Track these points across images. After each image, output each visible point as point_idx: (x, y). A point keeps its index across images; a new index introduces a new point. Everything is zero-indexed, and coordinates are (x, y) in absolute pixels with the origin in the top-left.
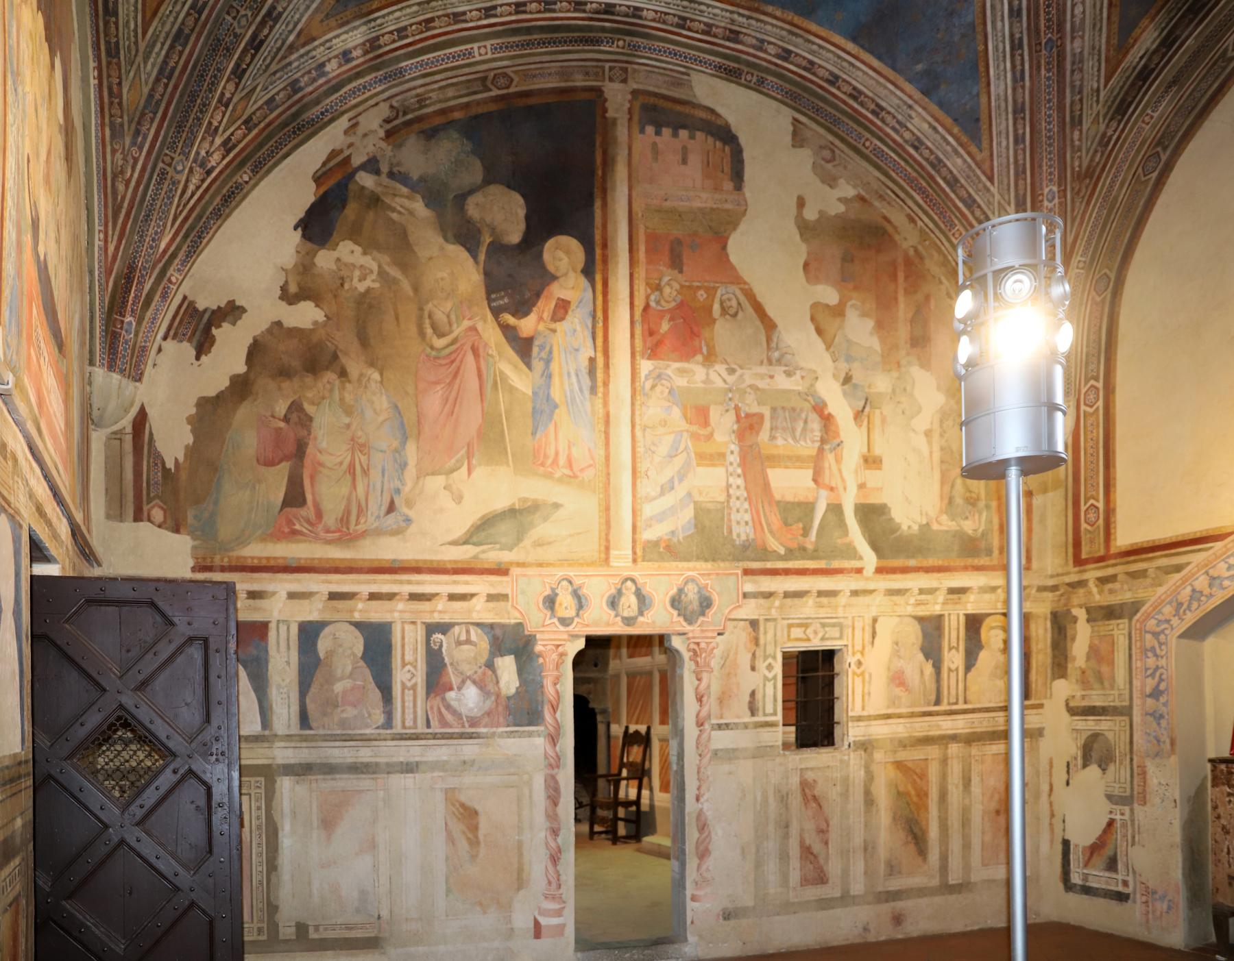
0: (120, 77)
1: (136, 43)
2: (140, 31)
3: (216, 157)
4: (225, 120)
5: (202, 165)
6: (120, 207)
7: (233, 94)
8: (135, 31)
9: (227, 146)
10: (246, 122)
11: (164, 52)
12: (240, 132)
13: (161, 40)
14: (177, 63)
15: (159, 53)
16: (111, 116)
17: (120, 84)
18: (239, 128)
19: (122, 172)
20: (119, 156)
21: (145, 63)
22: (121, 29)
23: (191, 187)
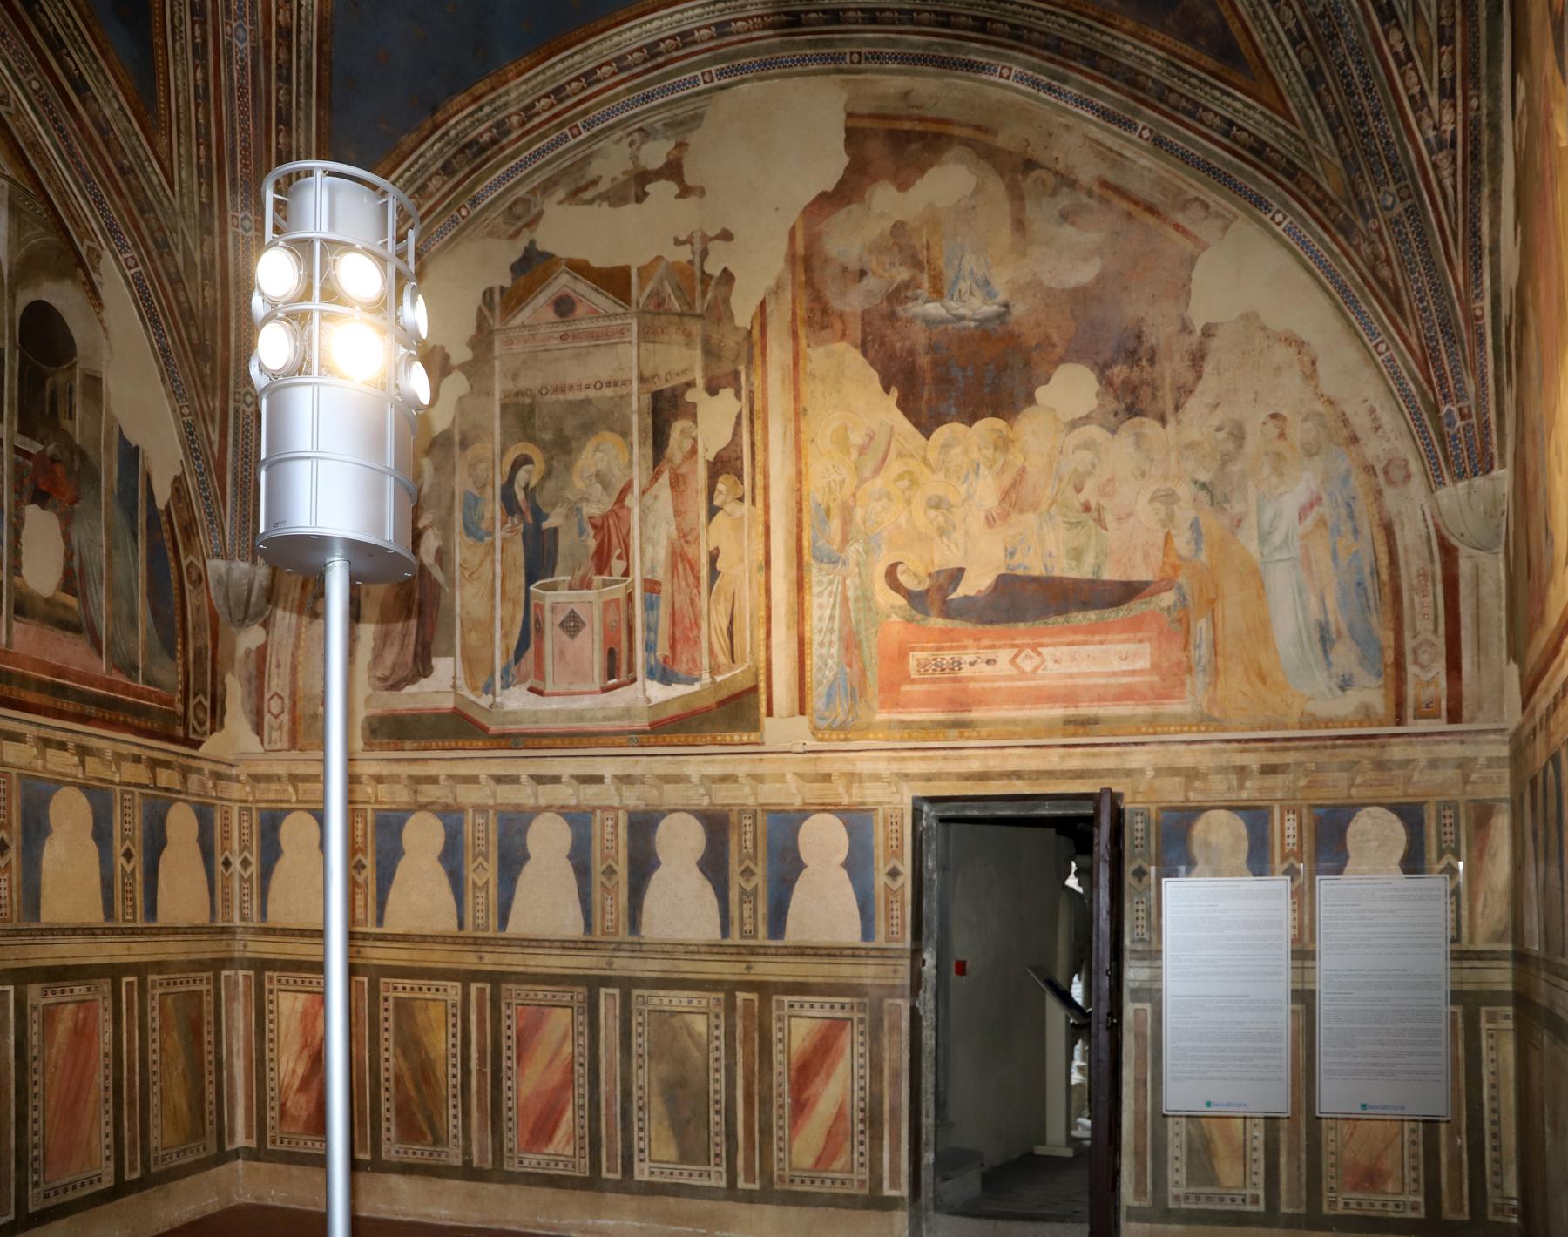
0: (1314, 182)
1: (1298, 138)
2: (1290, 126)
3: (1447, 117)
4: (1422, 72)
5: (1441, 145)
6: (1397, 290)
7: (1404, 39)
8: (1288, 131)
9: (1447, 92)
10: (1441, 41)
11: (1319, 111)
12: (1445, 58)
13: (1307, 105)
14: (1334, 102)
15: (1316, 115)
16: (1333, 221)
17: (1319, 187)
18: (1441, 55)
19: (1376, 258)
20: (1364, 247)
21: (1316, 140)
22: (1278, 147)
23: (1448, 182)
